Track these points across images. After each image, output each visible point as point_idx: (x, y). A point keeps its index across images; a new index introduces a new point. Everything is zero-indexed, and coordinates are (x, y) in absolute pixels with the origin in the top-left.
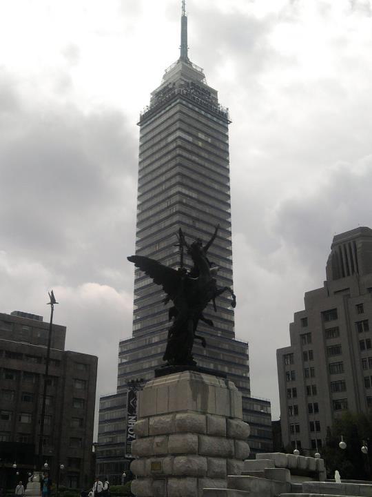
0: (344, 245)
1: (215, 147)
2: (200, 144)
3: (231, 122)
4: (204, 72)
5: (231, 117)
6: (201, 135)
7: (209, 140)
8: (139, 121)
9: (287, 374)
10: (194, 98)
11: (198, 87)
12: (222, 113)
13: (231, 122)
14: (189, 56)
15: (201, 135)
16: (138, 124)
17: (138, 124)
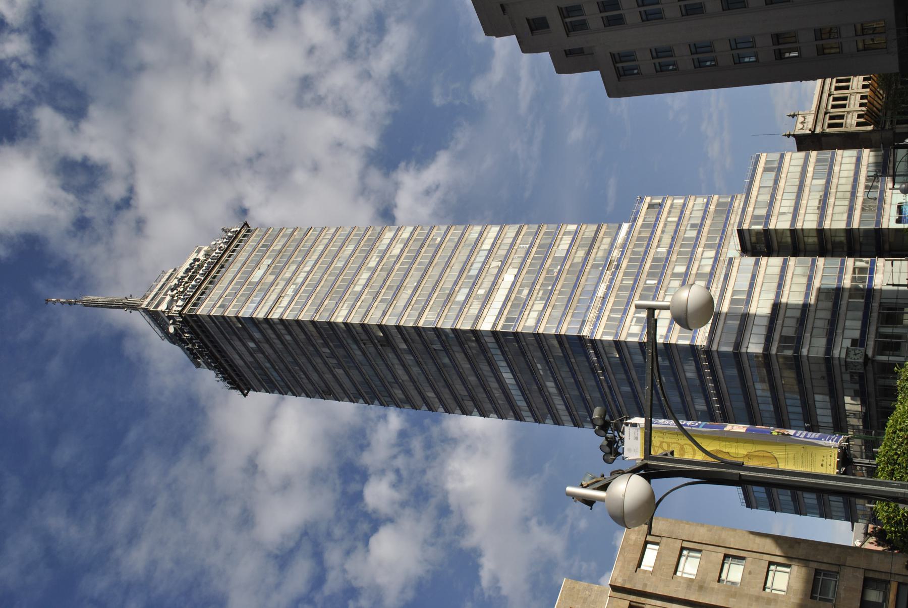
8: (239, 392)
9: (661, 69)
10: (194, 287)
16: (245, 395)
17: (245, 395)
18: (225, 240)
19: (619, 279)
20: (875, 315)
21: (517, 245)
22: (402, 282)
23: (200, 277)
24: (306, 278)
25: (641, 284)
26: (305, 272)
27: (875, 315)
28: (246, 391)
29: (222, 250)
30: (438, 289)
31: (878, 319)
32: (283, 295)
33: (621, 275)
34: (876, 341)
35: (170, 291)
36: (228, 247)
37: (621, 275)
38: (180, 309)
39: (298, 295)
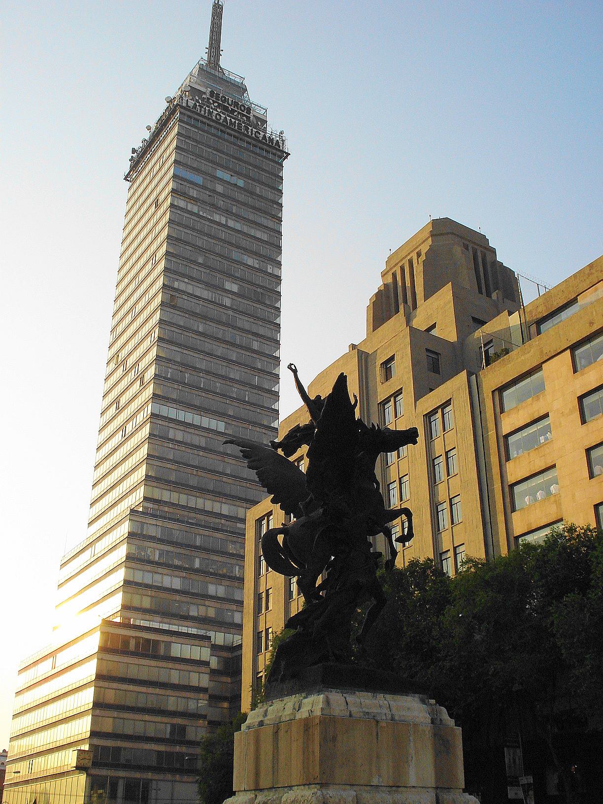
0: (402, 269)
1: (252, 193)
2: (219, 188)
3: (288, 154)
4: (245, 83)
5: (288, 147)
6: (220, 174)
7: (241, 183)
10: (210, 113)
11: (225, 100)
12: (271, 140)
13: (288, 154)
14: (222, 63)
15: (220, 174)
16: (126, 179)
17: (126, 179)
18: (268, 135)
19: (201, 532)
20: (138, 775)
21: (254, 428)
22: (212, 320)
23: (222, 118)
24: (219, 224)
25: (196, 554)
26: (226, 221)
27: (138, 775)
28: (129, 179)
29: (255, 135)
30: (201, 357)
31: (131, 778)
32: (199, 204)
33: (207, 533)
34: (140, 779)
35: (210, 90)
36: (260, 142)
37: (207, 533)
38: (184, 105)
39: (197, 219)
